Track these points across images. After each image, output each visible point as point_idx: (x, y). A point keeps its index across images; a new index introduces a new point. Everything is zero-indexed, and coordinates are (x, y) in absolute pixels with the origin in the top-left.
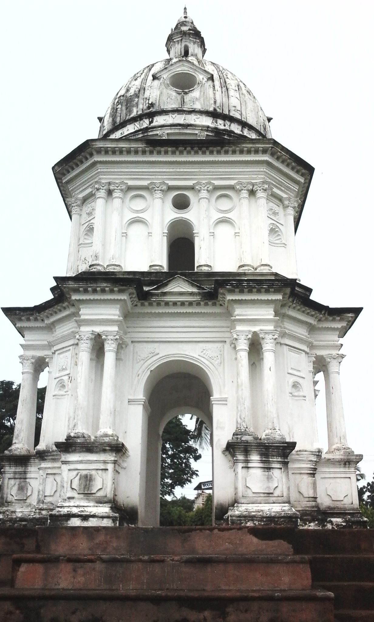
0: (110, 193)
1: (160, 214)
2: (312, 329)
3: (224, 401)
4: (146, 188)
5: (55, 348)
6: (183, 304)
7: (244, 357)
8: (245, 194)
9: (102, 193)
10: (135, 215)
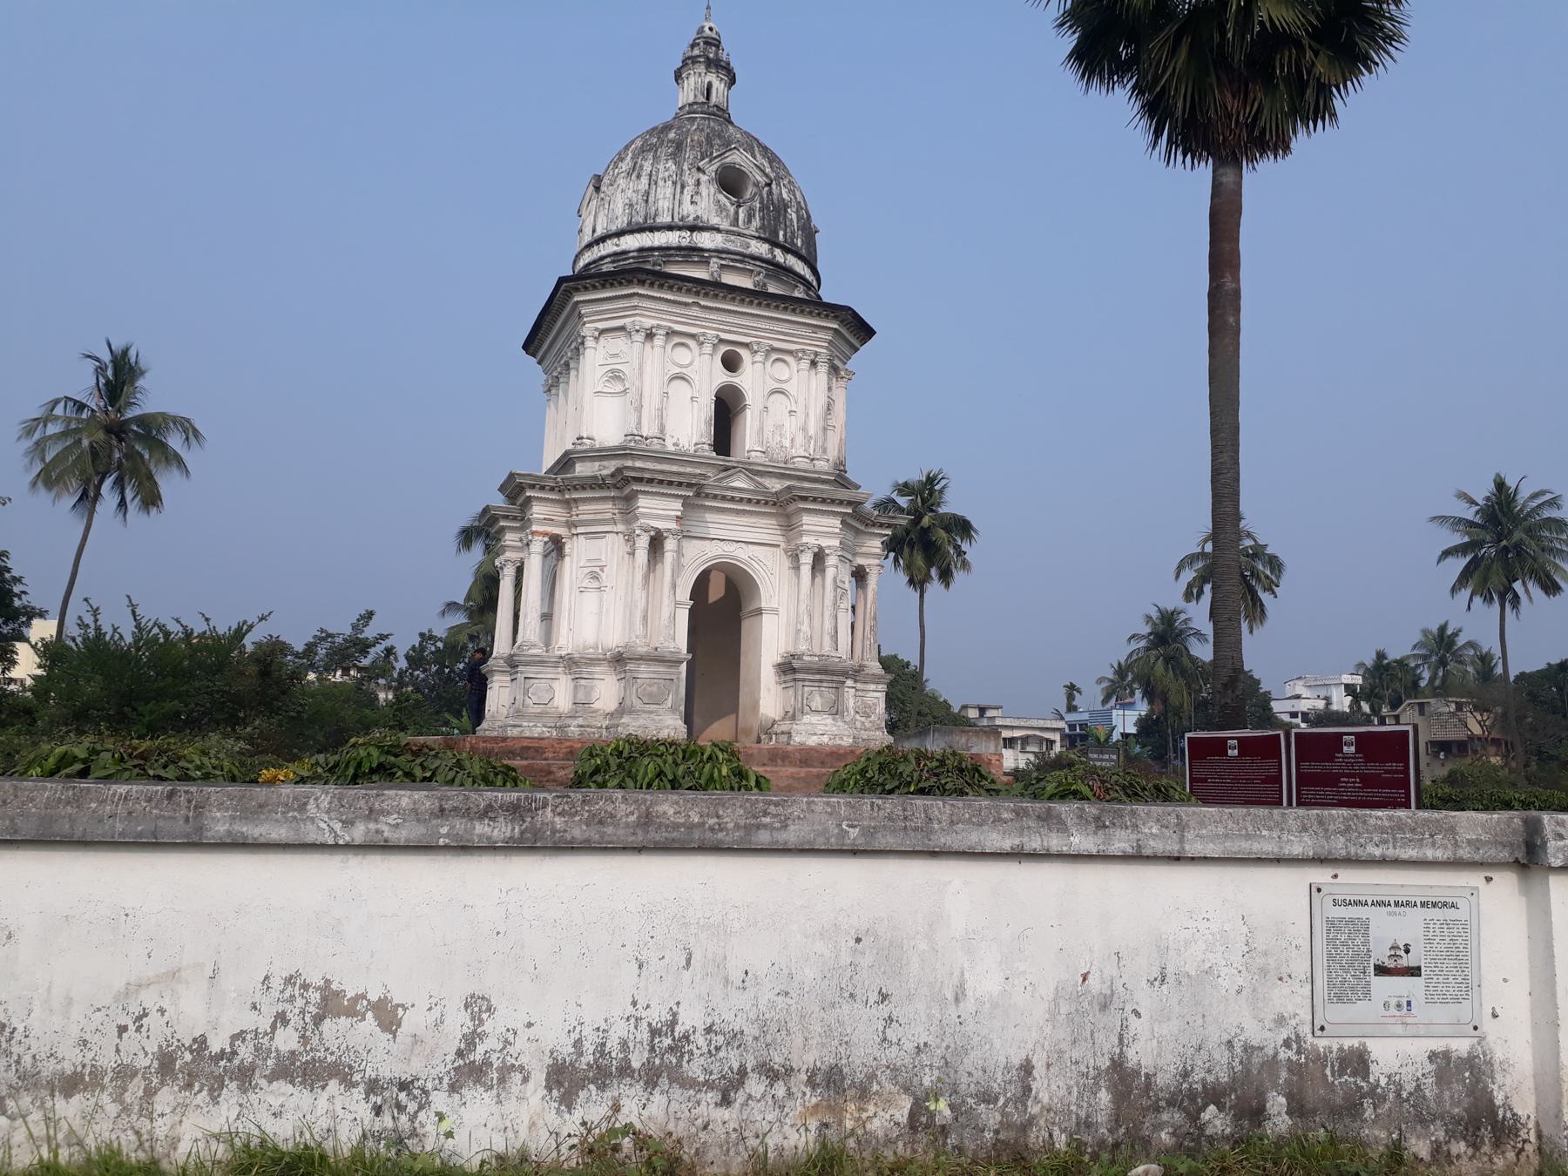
0: (650, 336)
1: (709, 376)
2: (858, 532)
3: (775, 611)
4: (693, 336)
5: (580, 530)
6: (741, 500)
7: (806, 570)
8: (805, 364)
9: (640, 337)
10: (678, 370)
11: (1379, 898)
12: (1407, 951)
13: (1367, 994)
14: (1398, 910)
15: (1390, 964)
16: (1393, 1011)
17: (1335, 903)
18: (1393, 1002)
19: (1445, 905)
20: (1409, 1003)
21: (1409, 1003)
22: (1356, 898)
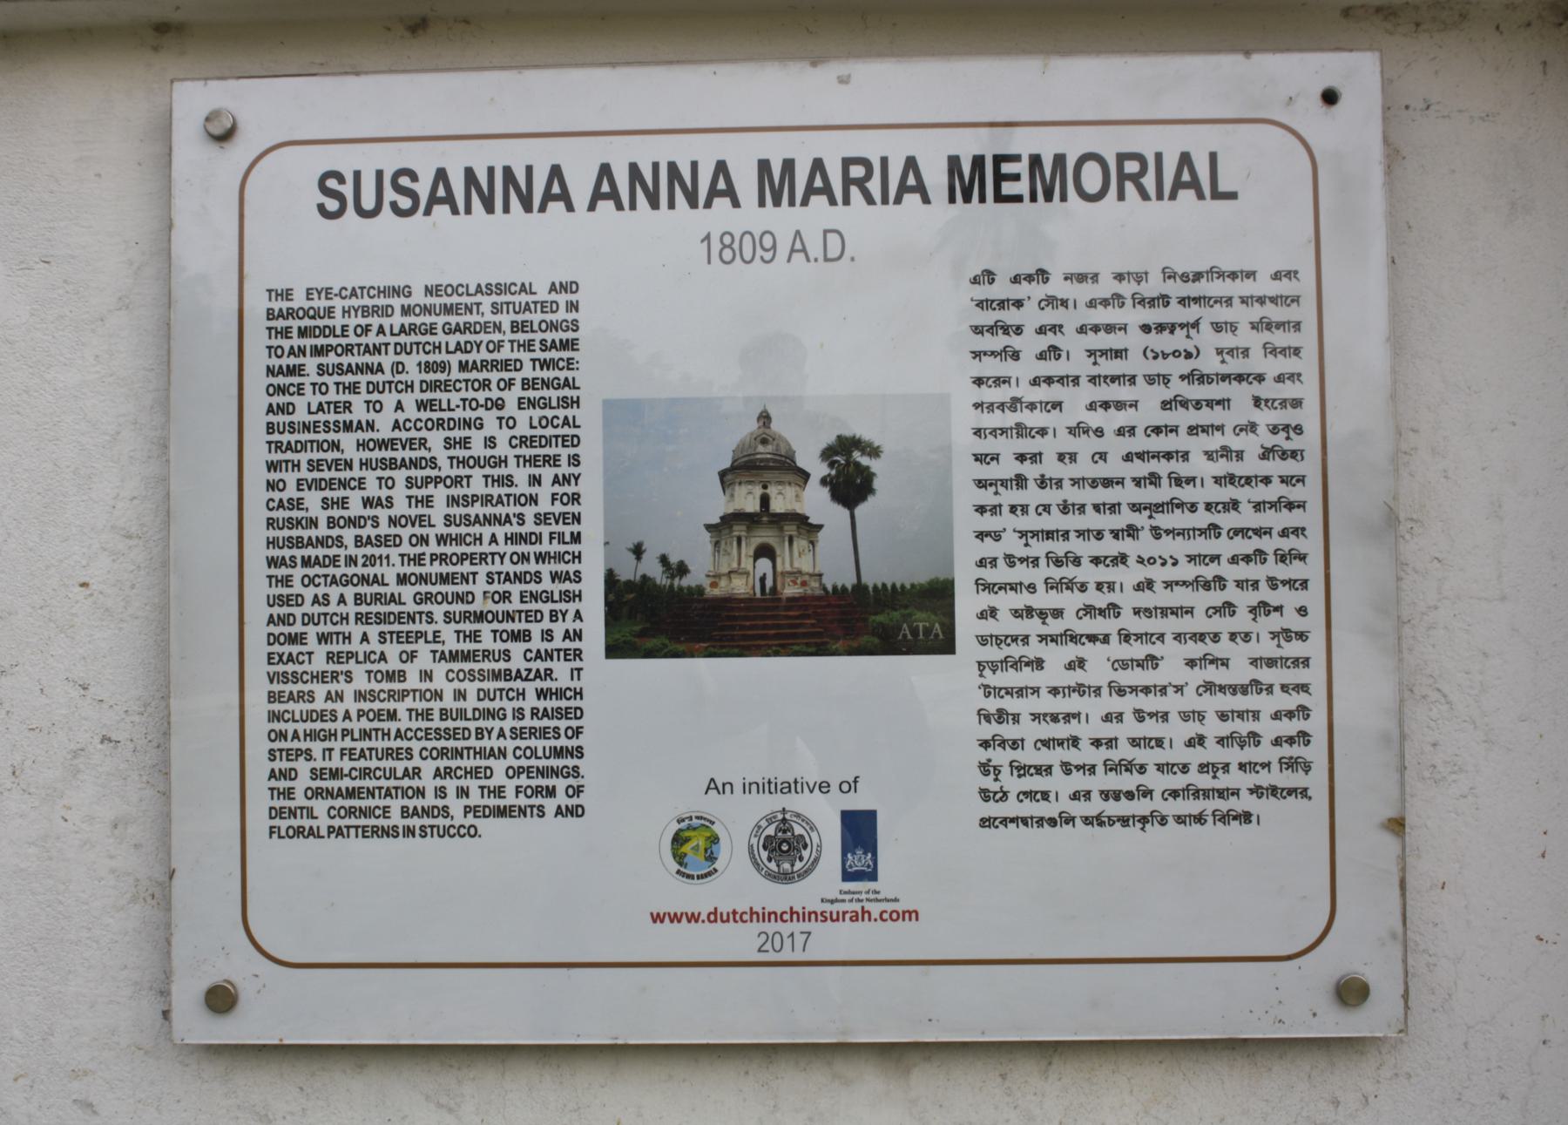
11: (646, 153)
12: (851, 486)
13: (553, 776)
14: (783, 220)
15: (739, 575)
16: (739, 879)
17: (336, 197)
18: (739, 821)
19: (1127, 175)
20: (860, 830)
21: (860, 830)
22: (483, 158)
